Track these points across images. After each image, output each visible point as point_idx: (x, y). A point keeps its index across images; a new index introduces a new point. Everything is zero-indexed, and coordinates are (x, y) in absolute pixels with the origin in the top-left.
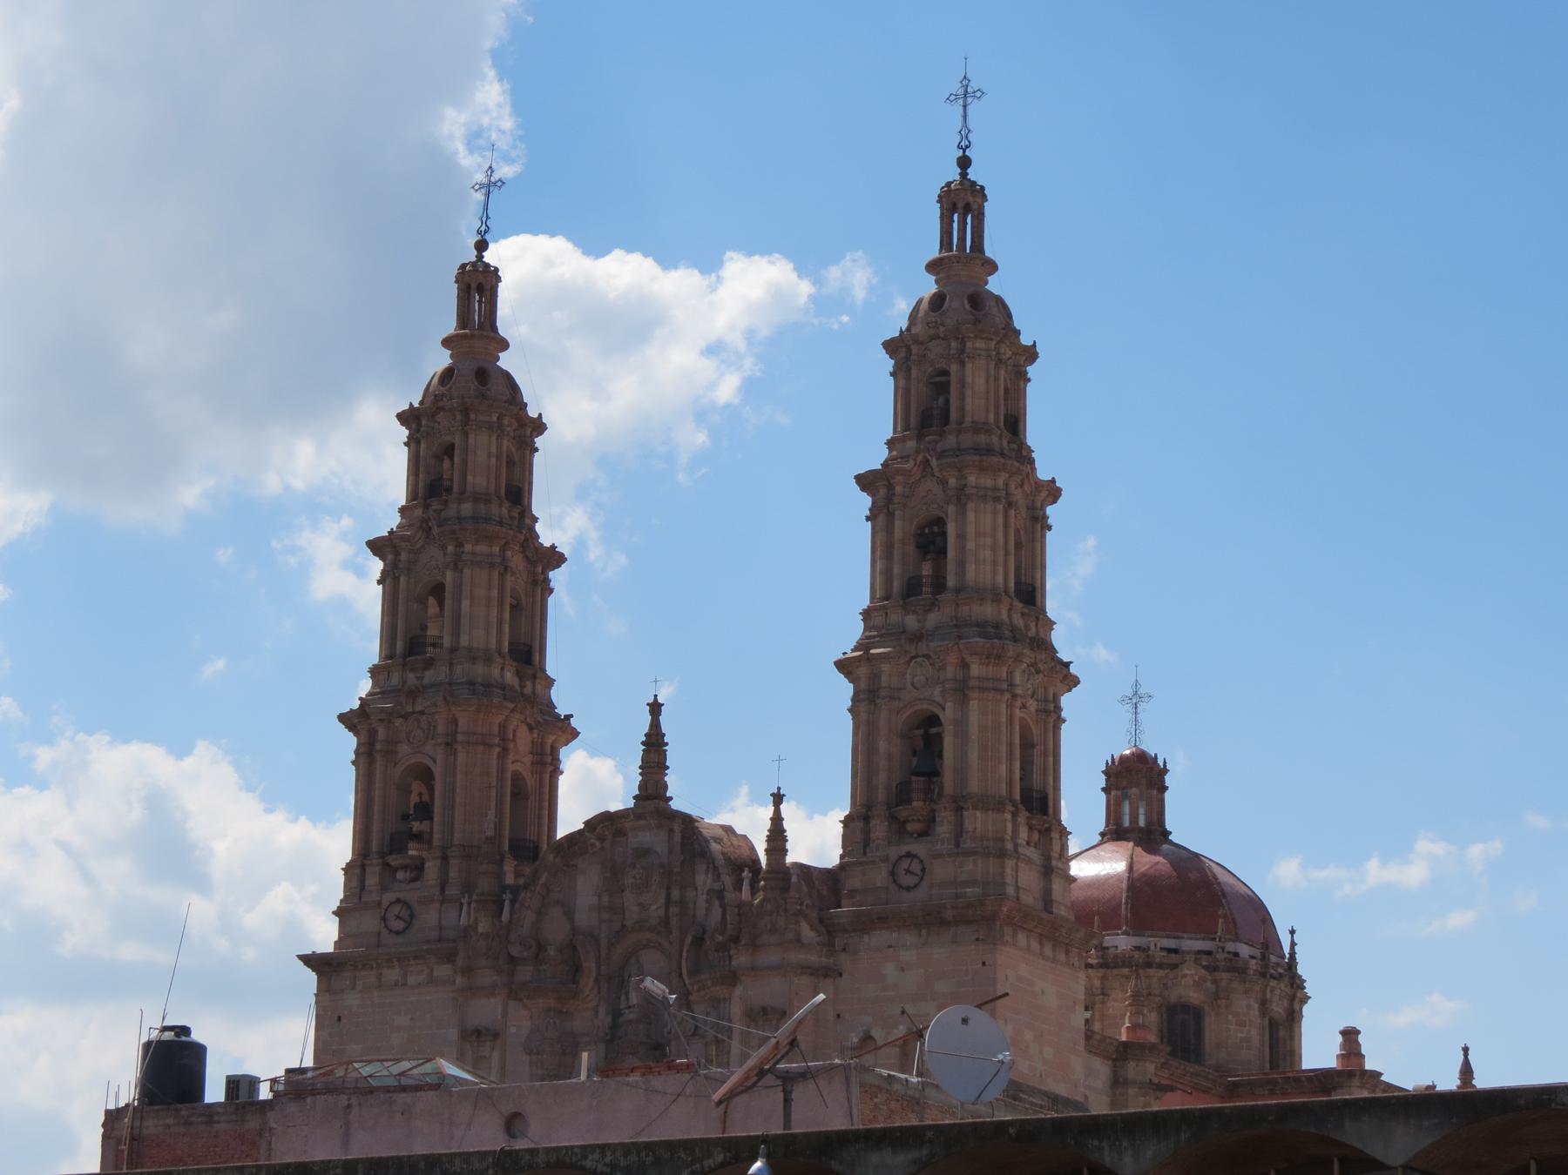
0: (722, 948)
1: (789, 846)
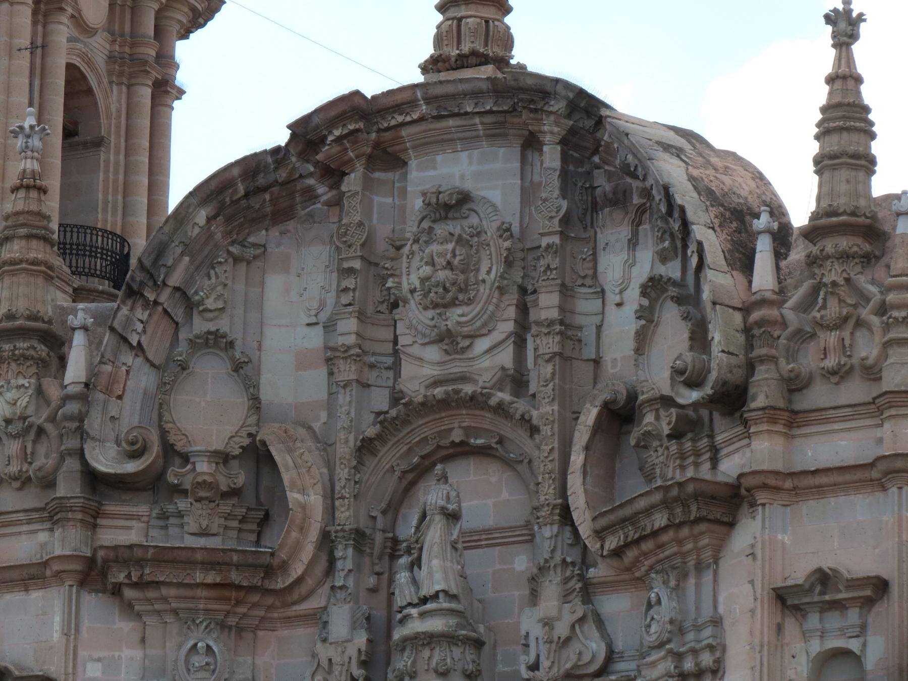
0: (687, 427)
1: (876, 148)
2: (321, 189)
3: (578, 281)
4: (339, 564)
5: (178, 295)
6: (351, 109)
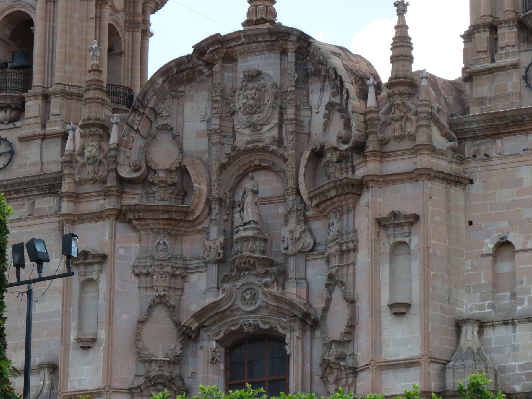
0: (343, 158)
1: (413, 53)
2: (205, 70)
3: (302, 104)
4: (213, 211)
5: (152, 110)
6: (216, 40)
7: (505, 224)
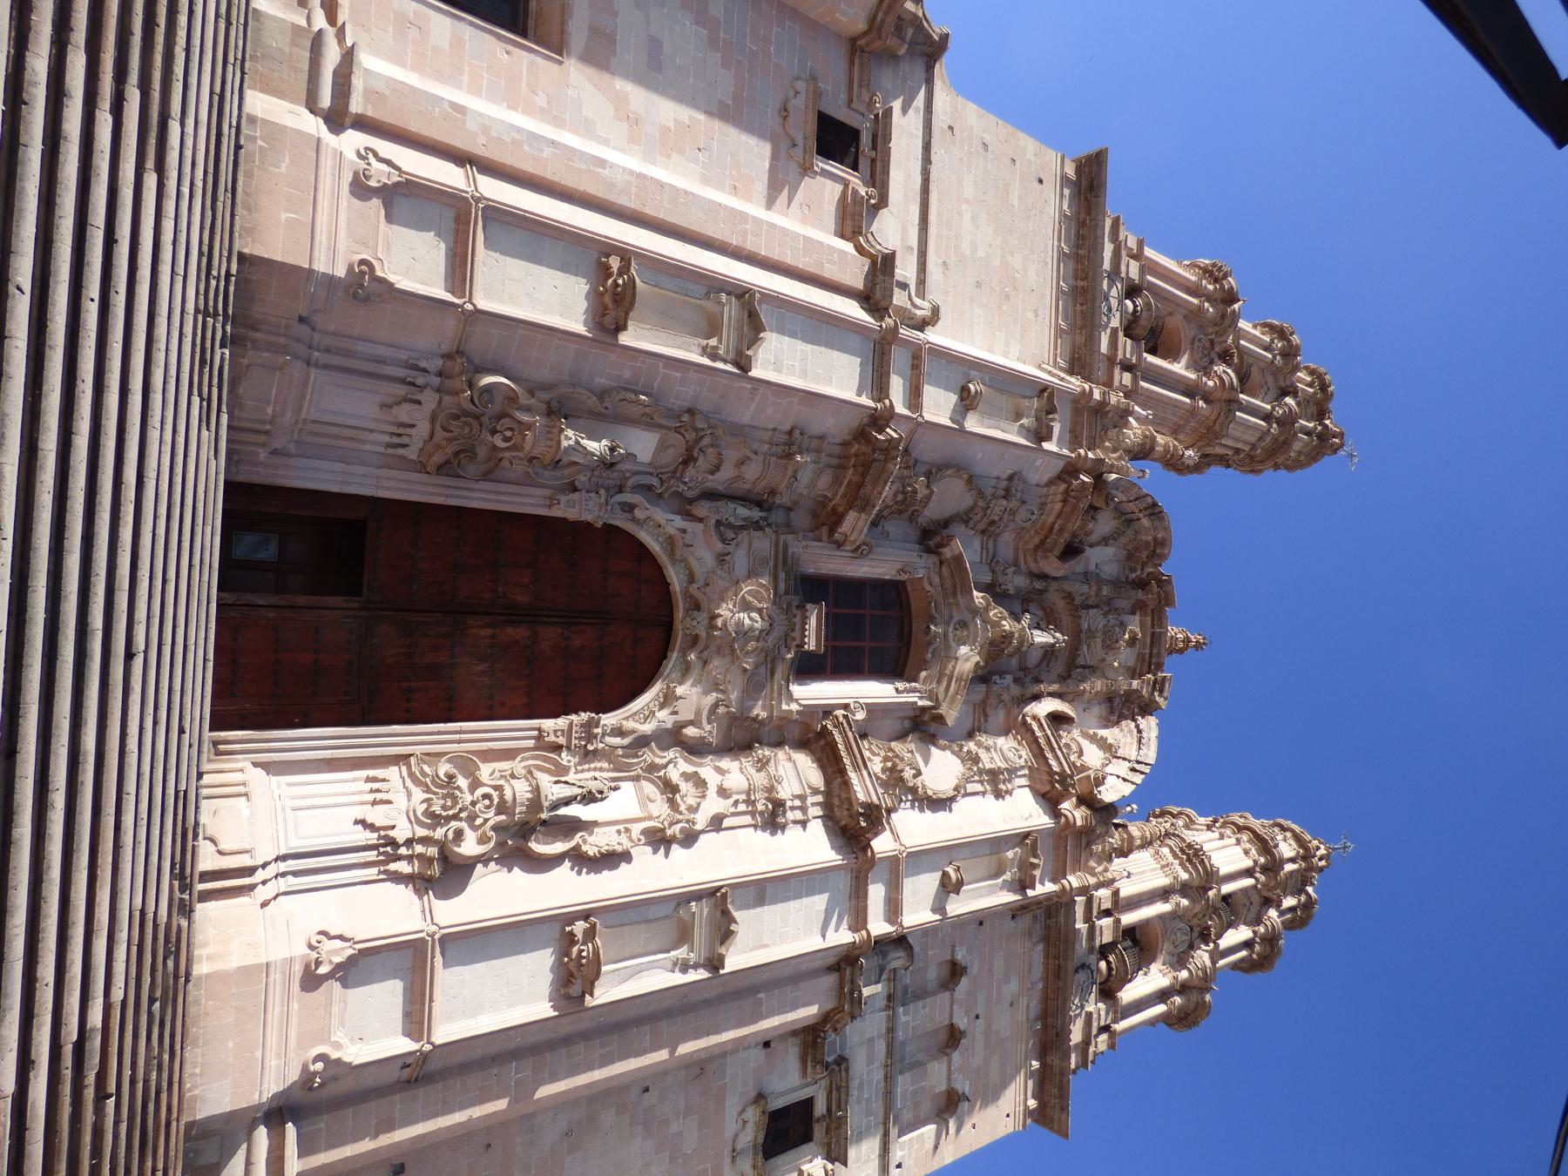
7: (975, 972)
